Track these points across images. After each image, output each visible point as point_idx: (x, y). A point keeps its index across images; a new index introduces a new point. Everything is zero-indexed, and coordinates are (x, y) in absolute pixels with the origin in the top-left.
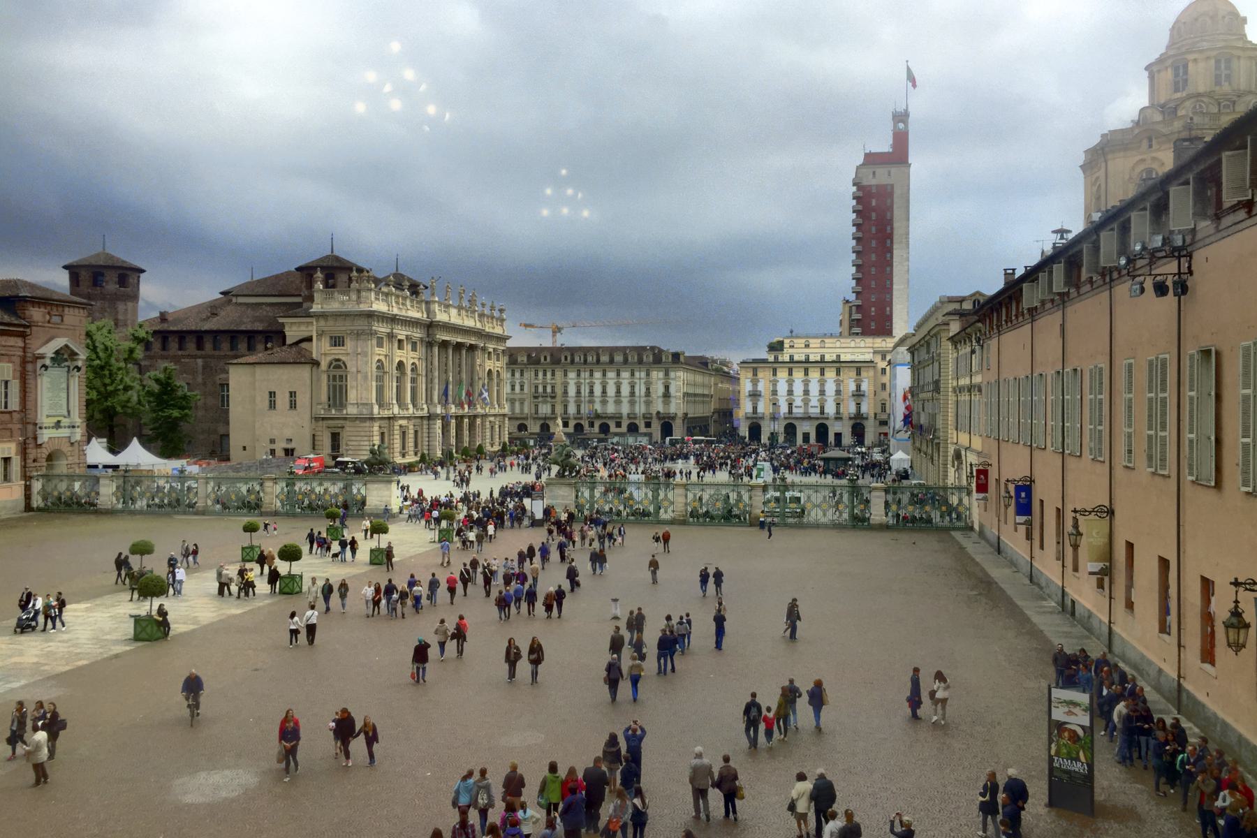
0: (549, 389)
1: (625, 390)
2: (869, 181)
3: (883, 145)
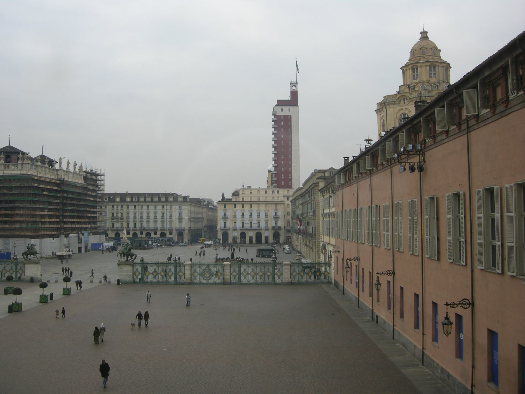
0: (120, 215)
1: (159, 215)
2: (279, 113)
3: (287, 97)
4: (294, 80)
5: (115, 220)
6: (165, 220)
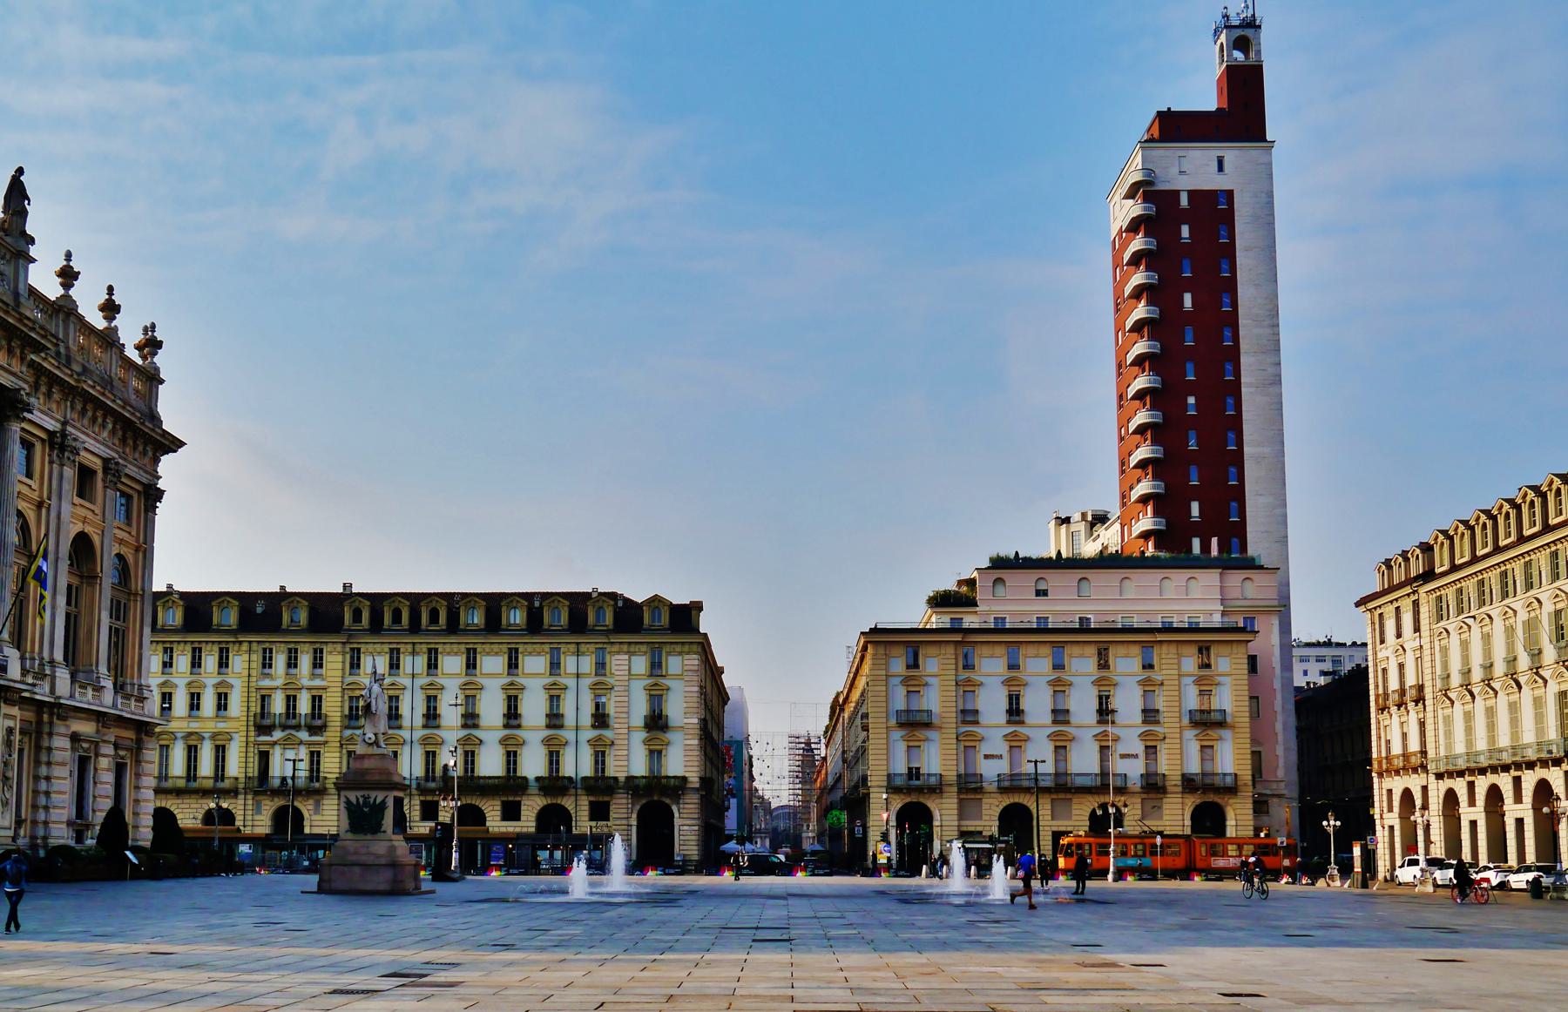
0: (304, 707)
1: (534, 709)
3: (1205, 97)
4: (1237, 11)
5: (278, 735)
6: (568, 735)
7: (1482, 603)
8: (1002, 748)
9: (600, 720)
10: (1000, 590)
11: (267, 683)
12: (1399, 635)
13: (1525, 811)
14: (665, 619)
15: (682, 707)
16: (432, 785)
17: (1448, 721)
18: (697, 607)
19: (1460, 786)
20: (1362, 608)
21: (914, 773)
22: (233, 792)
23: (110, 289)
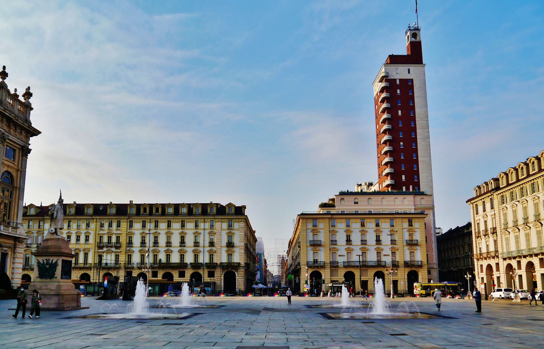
0: (114, 240)
1: (190, 240)
3: (403, 50)
4: (413, 25)
5: (105, 249)
6: (201, 249)
7: (522, 196)
8: (345, 253)
9: (212, 244)
10: (343, 202)
11: (102, 232)
12: (484, 211)
13: (523, 272)
14: (233, 211)
15: (239, 240)
16: (156, 266)
17: (507, 240)
18: (244, 207)
19: (514, 263)
20: (469, 203)
21: (315, 261)
22: (90, 268)
23: (4, 67)
